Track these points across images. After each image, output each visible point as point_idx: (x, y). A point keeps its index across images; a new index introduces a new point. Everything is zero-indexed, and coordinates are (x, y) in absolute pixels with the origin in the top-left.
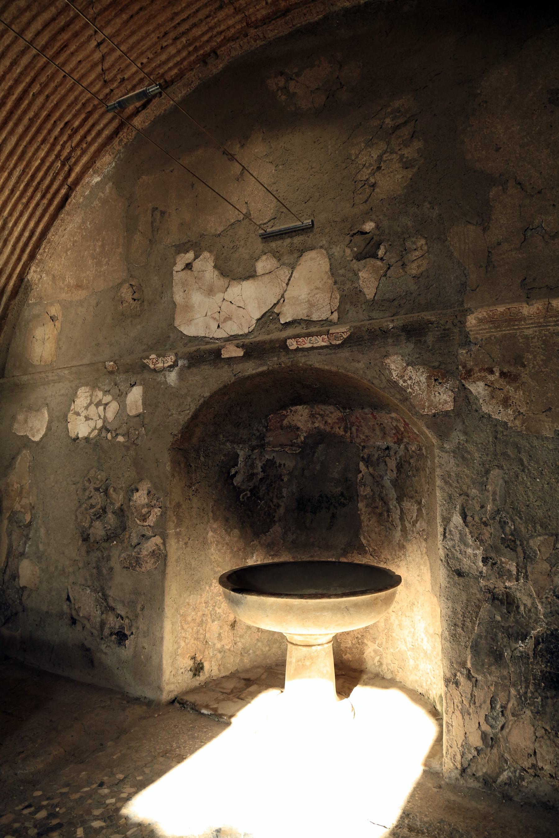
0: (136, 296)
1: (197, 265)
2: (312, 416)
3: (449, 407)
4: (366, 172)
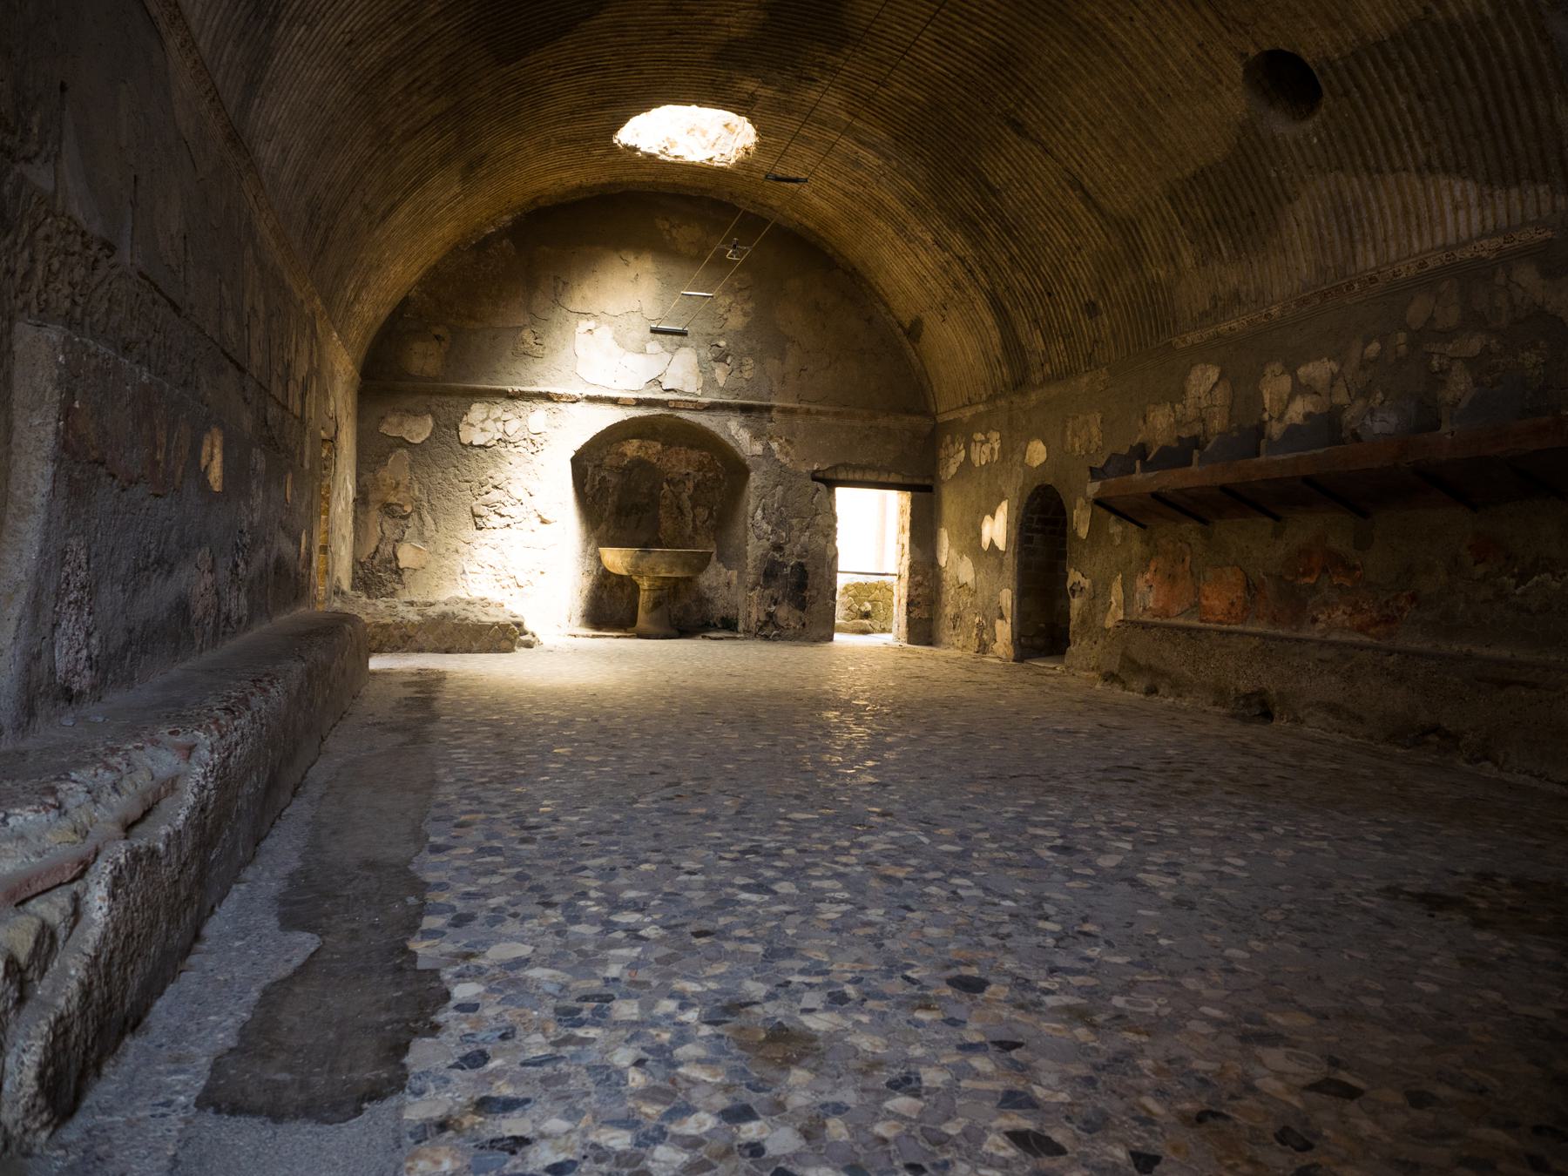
0: (538, 341)
1: (595, 332)
2: (640, 447)
3: (760, 453)
4: (721, 311)
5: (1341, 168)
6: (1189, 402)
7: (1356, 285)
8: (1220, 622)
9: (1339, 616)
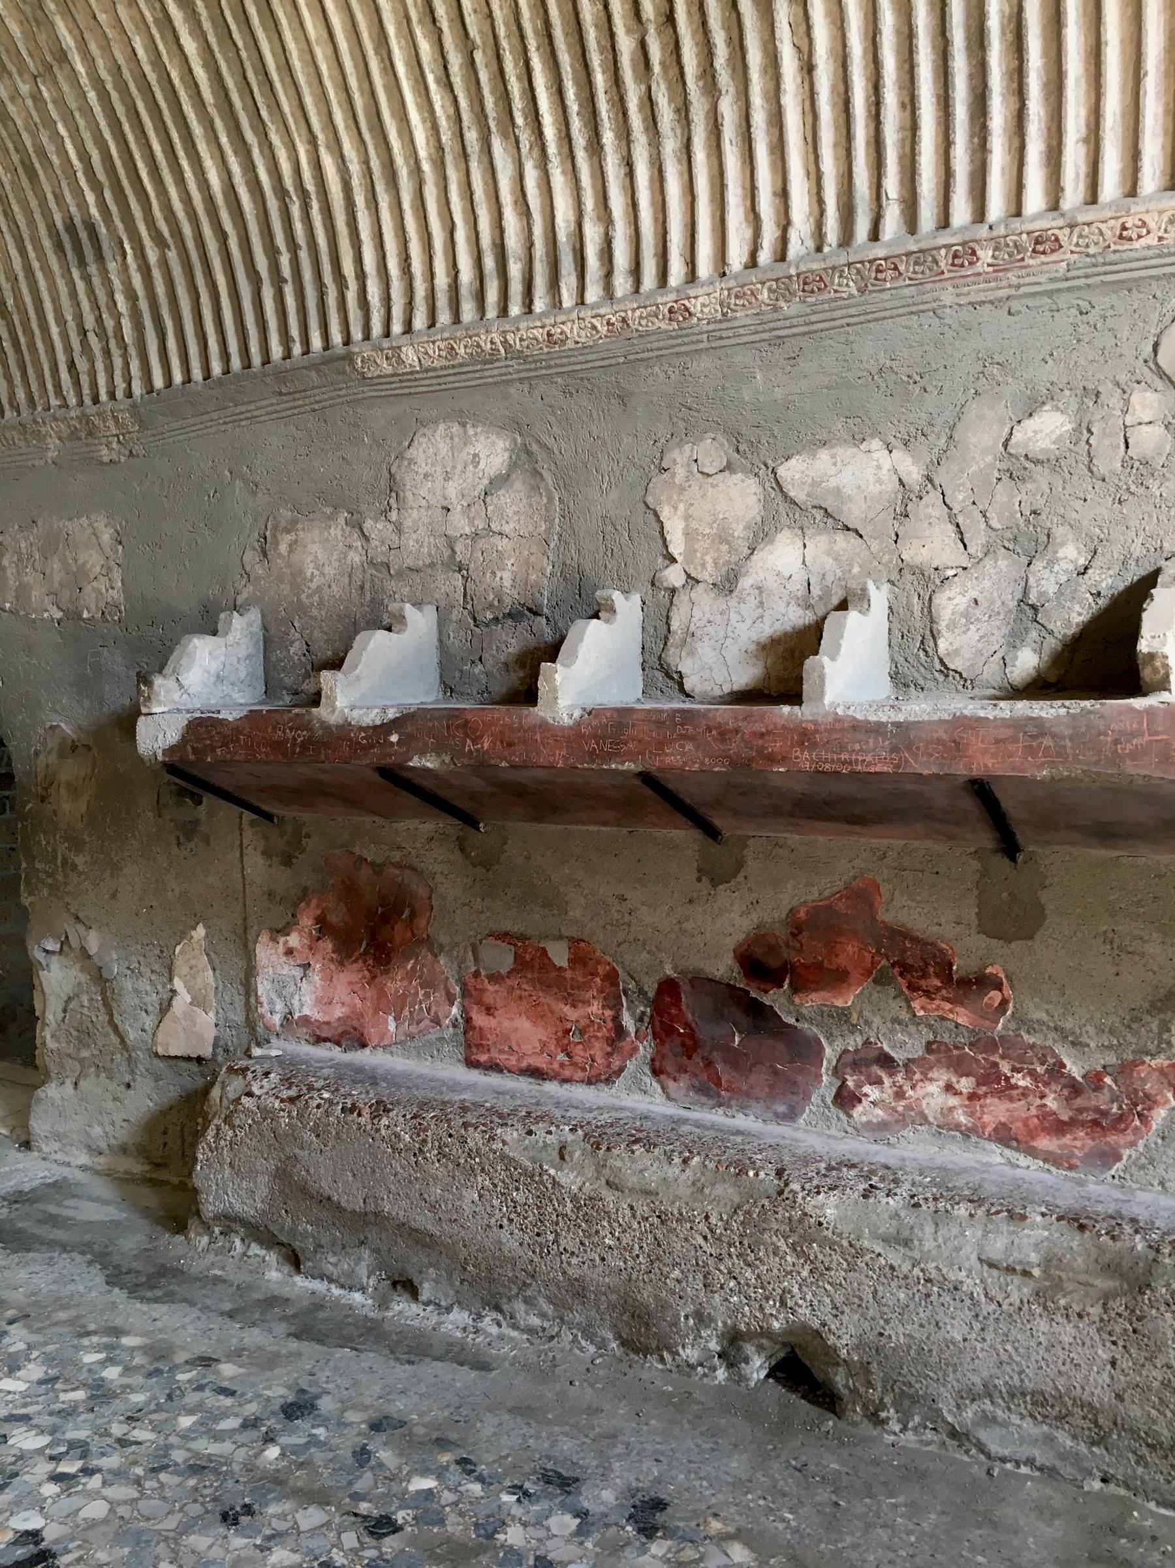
7: (986, 255)
8: (536, 1073)
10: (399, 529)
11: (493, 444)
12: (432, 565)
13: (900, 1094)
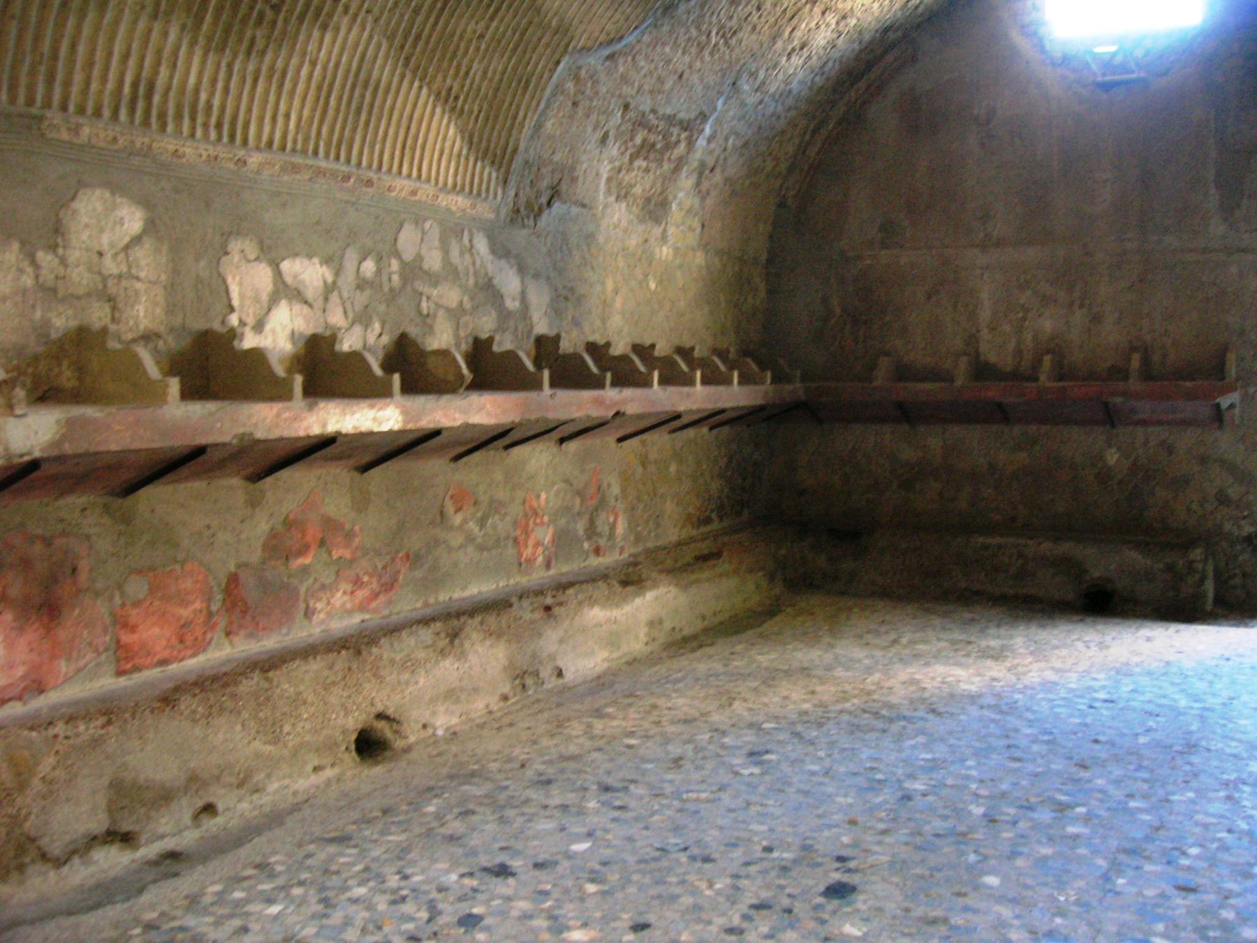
5: (391, 39)
6: (74, 255)
9: (339, 599)
10: (63, 262)
11: (133, 213)
12: (89, 295)
13: (329, 603)
